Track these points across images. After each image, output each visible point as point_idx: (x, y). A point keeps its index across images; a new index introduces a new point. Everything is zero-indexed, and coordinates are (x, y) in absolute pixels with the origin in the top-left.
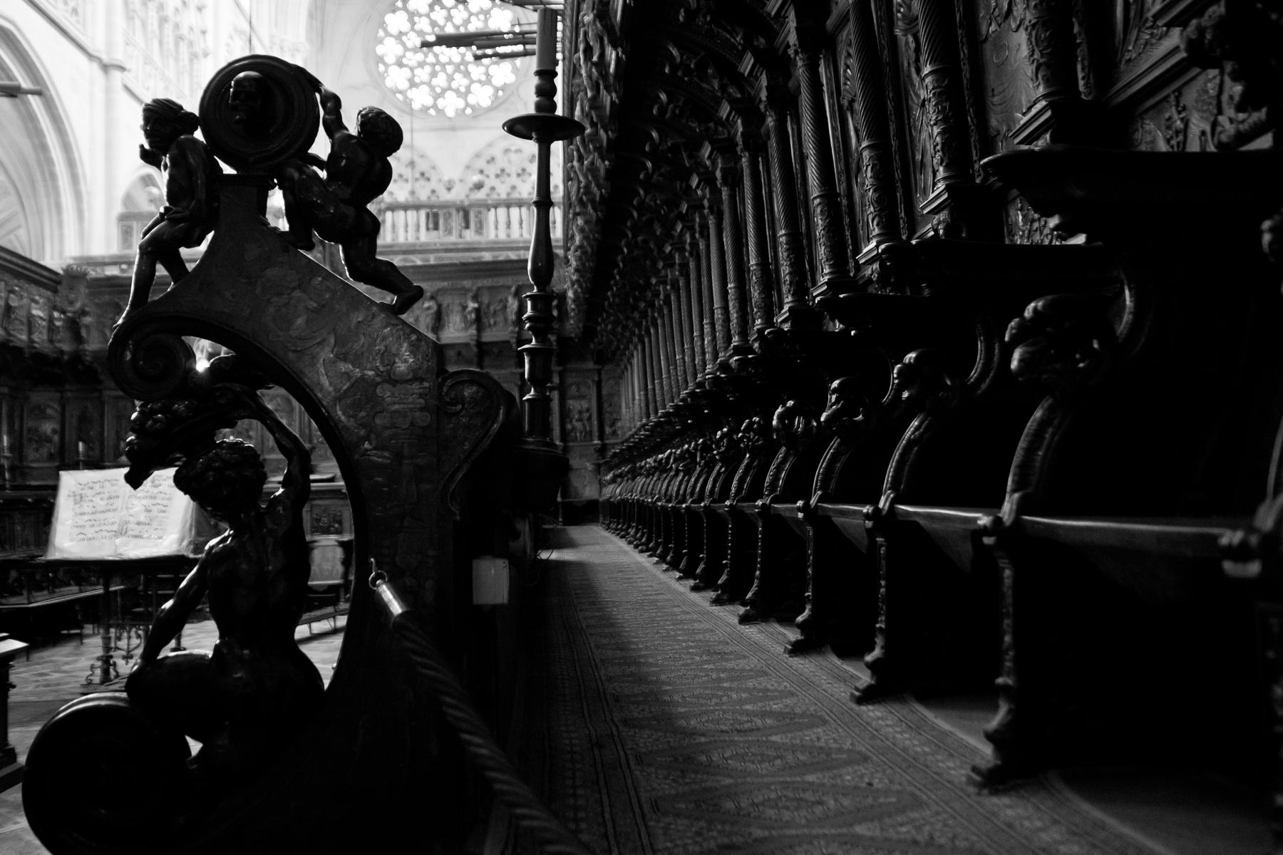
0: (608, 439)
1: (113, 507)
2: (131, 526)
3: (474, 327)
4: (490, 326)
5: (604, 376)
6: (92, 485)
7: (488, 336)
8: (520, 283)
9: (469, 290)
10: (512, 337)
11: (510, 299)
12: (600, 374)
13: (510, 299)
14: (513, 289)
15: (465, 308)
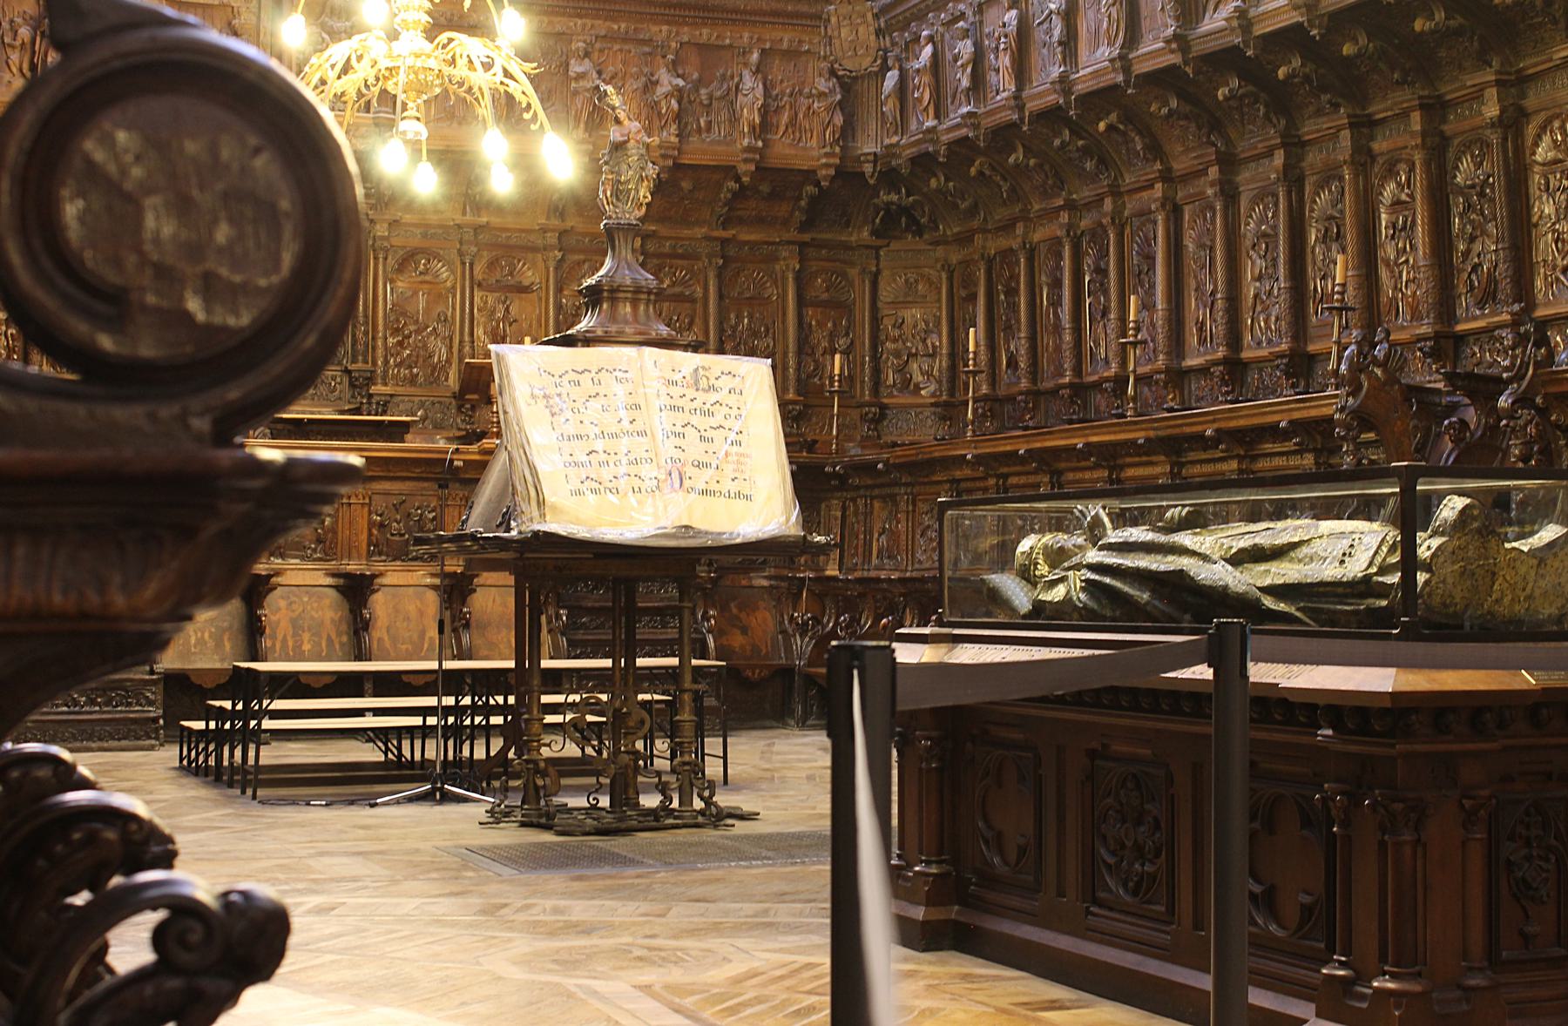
0: (891, 396)
1: (638, 426)
2: (690, 471)
3: (673, 128)
4: (699, 130)
5: (881, 266)
6: (575, 377)
7: (701, 151)
8: (768, 46)
9: (664, 47)
10: (746, 161)
11: (748, 81)
12: (877, 258)
13: (748, 81)
14: (755, 56)
15: (650, 85)
